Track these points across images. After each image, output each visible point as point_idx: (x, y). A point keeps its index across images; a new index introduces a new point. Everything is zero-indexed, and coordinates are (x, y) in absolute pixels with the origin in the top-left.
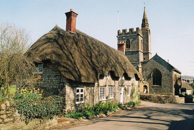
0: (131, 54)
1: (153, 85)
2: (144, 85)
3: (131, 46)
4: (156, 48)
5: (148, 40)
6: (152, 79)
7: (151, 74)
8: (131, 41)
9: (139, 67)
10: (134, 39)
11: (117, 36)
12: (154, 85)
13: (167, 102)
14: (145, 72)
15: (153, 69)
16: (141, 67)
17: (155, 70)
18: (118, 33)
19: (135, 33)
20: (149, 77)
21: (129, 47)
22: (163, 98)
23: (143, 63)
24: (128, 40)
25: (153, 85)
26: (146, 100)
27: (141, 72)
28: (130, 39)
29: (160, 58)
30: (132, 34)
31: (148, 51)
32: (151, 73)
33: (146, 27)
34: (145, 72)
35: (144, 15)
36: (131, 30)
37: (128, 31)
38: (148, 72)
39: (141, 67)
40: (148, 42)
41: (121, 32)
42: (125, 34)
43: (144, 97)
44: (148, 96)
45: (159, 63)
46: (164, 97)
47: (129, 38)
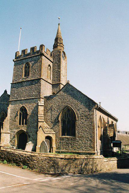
0: (29, 85)
1: (62, 135)
2: (46, 135)
3: (30, 72)
4: (71, 75)
5: (60, 65)
6: (60, 124)
7: (58, 116)
8: (31, 65)
9: (39, 104)
10: (36, 62)
11: (13, 60)
12: (64, 136)
13: (71, 171)
14: (49, 114)
15: (62, 108)
16: (43, 104)
17: (66, 110)
18: (16, 55)
19: (38, 52)
20: (56, 122)
21: (28, 75)
22: (61, 163)
23: (48, 98)
24: (28, 64)
25: (62, 135)
26: (24, 165)
27: (43, 113)
28: (31, 62)
29: (74, 89)
30: (33, 54)
31: (60, 80)
32: (59, 115)
33: (59, 48)
34: (49, 114)
35: (58, 33)
36: (33, 49)
37: (29, 51)
38: (55, 113)
39: (43, 104)
40: (60, 69)
41: (20, 53)
42: (24, 56)
43: (20, 159)
44: (28, 157)
45: (72, 96)
46: (62, 159)
47: (29, 60)
